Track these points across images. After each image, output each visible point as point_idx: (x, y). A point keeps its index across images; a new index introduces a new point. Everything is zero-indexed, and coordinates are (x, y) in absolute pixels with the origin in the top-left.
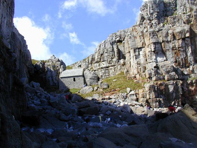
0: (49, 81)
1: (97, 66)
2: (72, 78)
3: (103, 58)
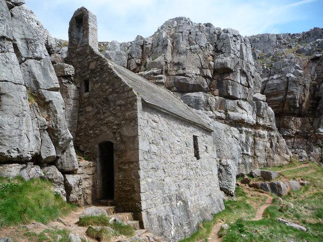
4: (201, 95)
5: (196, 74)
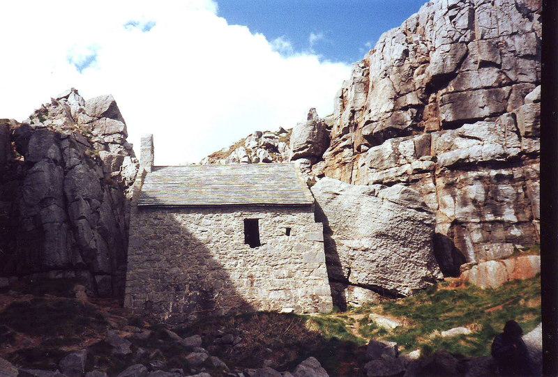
0: (41, 231)
1: (397, 156)
2: (235, 222)
3: (458, 101)
4: (388, 146)
5: (386, 112)
